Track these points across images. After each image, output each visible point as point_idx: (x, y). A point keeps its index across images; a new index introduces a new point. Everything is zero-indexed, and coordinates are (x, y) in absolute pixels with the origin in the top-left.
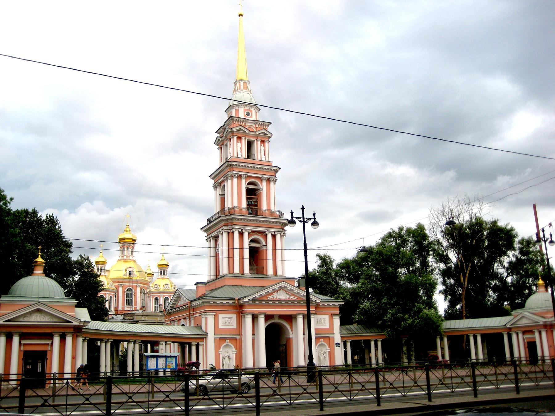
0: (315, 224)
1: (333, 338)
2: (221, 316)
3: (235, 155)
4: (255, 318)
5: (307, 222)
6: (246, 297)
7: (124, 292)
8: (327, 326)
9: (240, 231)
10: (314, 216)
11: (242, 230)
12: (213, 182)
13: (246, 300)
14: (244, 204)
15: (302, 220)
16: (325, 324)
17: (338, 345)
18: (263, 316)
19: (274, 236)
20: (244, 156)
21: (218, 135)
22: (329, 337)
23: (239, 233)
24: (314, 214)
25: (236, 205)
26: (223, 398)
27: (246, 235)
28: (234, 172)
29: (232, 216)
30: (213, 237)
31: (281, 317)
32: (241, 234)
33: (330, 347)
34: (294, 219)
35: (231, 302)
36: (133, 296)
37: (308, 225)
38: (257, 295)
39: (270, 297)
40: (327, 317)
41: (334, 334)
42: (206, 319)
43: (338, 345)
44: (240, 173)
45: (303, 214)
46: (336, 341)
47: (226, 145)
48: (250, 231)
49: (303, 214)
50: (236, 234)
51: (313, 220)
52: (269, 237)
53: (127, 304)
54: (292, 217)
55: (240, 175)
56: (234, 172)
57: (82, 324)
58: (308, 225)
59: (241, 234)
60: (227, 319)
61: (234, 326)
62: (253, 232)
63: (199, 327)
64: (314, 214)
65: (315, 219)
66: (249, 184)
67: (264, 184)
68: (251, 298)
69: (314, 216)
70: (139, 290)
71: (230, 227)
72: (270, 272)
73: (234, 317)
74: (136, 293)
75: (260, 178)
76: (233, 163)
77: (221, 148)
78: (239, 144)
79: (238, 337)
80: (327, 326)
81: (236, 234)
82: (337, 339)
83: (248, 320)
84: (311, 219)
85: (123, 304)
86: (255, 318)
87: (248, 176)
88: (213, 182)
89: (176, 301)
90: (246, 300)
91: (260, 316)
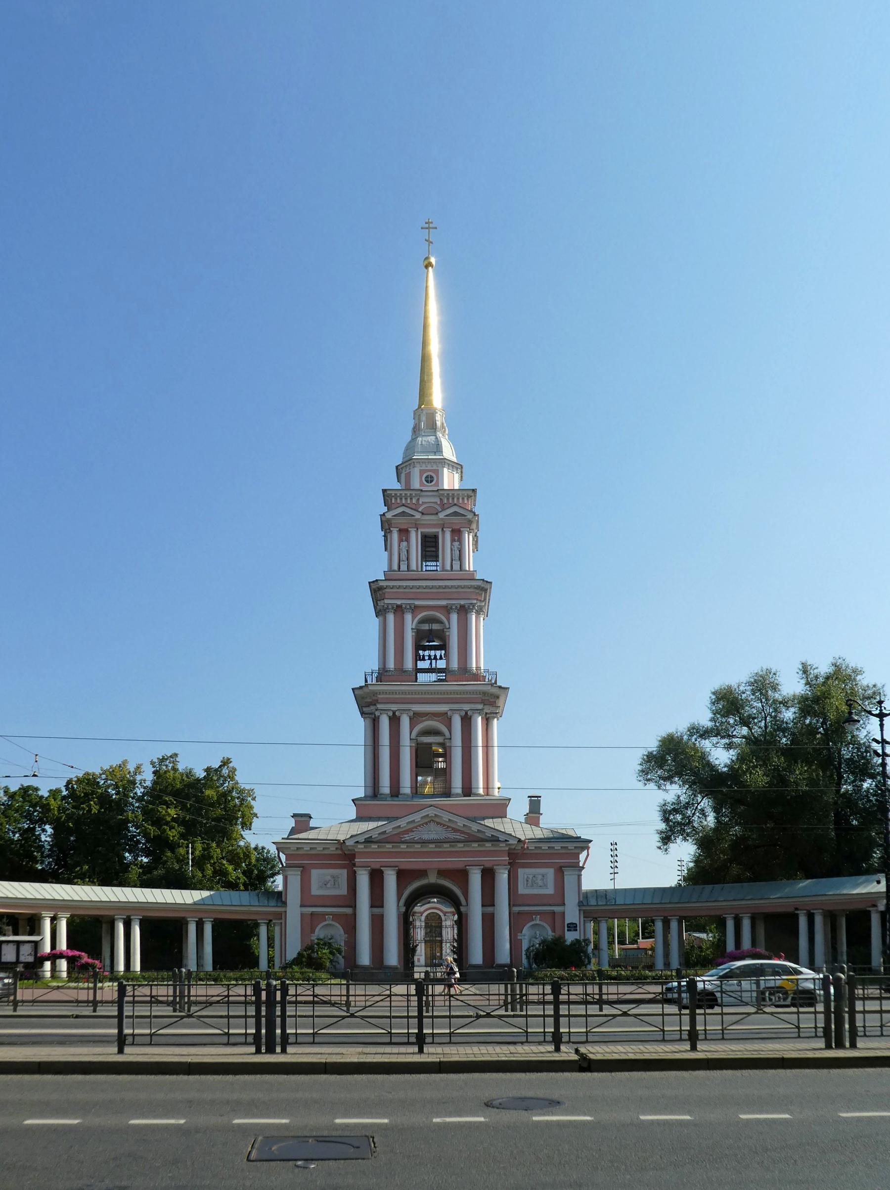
1: (563, 914)
2: (315, 873)
3: (395, 567)
8: (550, 890)
16: (545, 886)
22: (553, 913)
31: (442, 873)
32: (395, 720)
40: (550, 872)
44: (399, 602)
56: (386, 601)
60: (329, 878)
66: (422, 621)
67: (454, 617)
76: (381, 584)
79: (348, 911)
80: (550, 890)
87: (416, 607)
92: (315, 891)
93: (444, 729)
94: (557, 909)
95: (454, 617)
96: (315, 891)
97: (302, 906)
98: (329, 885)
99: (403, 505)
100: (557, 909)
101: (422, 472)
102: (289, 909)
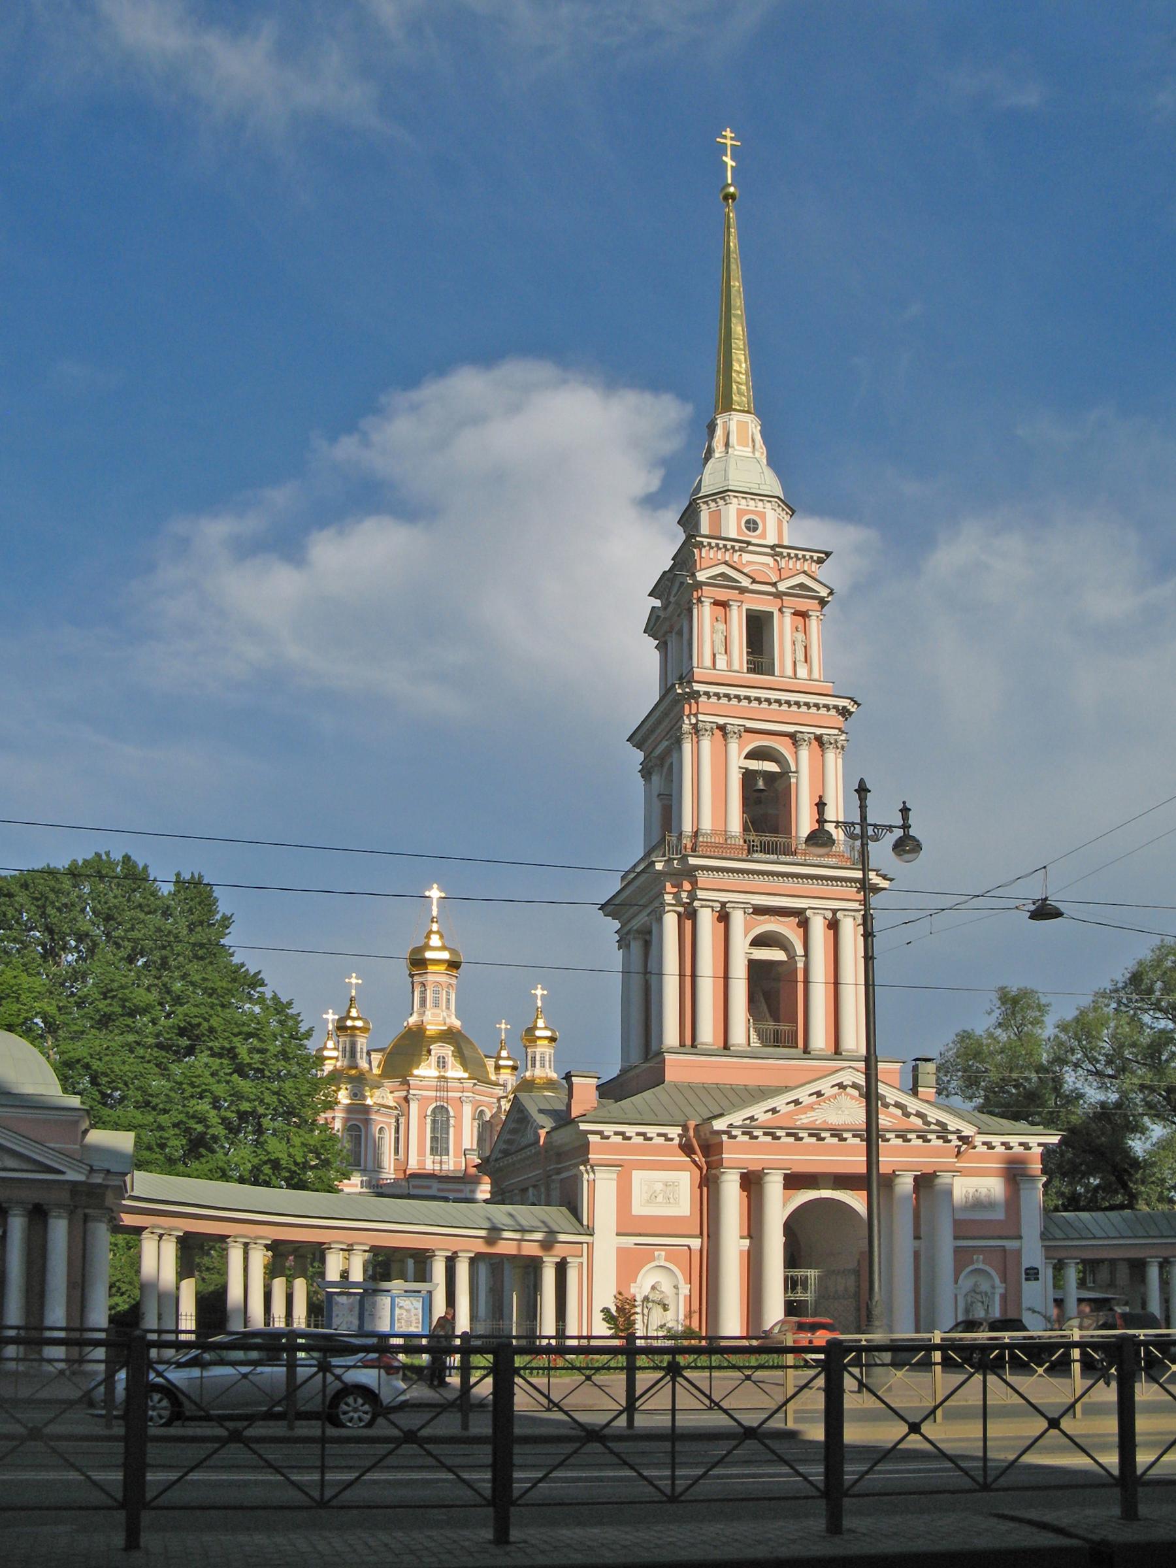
0: (906, 845)
1: (1018, 1252)
5: (876, 839)
6: (721, 1115)
10: (905, 818)
12: (640, 756)
14: (735, 824)
15: (858, 830)
17: (1032, 1274)
19: (833, 925)
20: (736, 667)
21: (658, 603)
22: (1003, 1249)
24: (905, 811)
26: (323, 1440)
27: (738, 919)
28: (701, 717)
29: (692, 861)
30: (638, 932)
32: (724, 917)
33: (1004, 1280)
34: (830, 827)
36: (452, 1130)
37: (881, 851)
39: (804, 1119)
41: (1020, 1237)
43: (1032, 1274)
45: (863, 808)
46: (1026, 1263)
47: (680, 633)
49: (863, 808)
50: (706, 918)
51: (899, 833)
52: (818, 926)
53: (433, 1151)
54: (821, 821)
55: (722, 728)
56: (701, 717)
57: (98, 1179)
58: (881, 851)
59: (724, 917)
62: (759, 911)
64: (905, 811)
65: (906, 827)
69: (905, 818)
70: (468, 1110)
72: (820, 1039)
75: (792, 736)
77: (666, 643)
78: (721, 626)
82: (1032, 1253)
84: (890, 828)
85: (421, 1152)
86: (752, 1183)
88: (640, 756)
90: (719, 1125)
91: (768, 1178)
92: (639, 1208)
93: (794, 937)
94: (1010, 1244)
95: (804, 753)
96: (639, 1208)
98: (660, 1199)
99: (726, 563)
100: (1010, 1244)
101: (741, 513)
102: (598, 1239)
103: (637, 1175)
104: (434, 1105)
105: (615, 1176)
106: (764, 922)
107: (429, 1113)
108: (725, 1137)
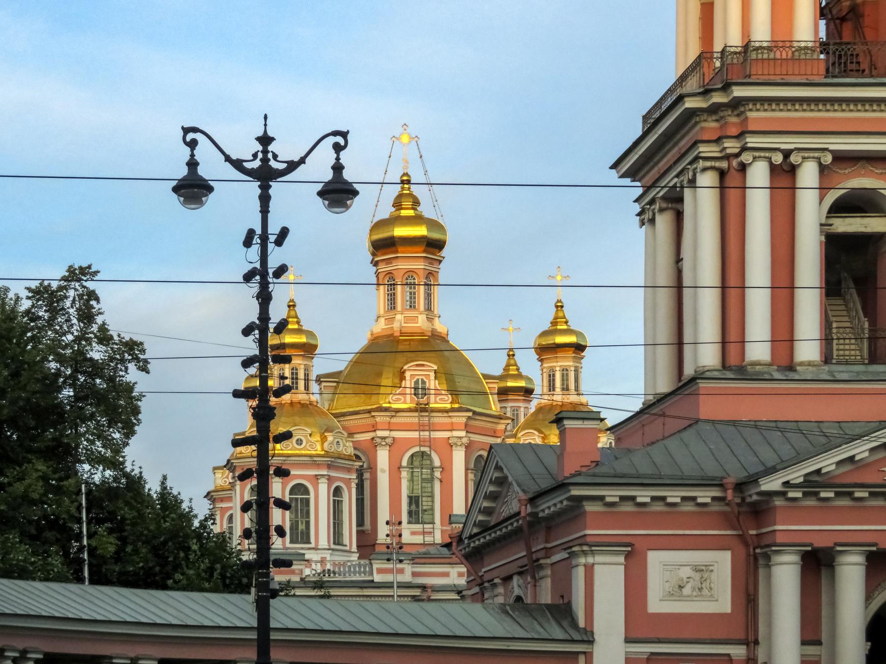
4: (818, 564)
7: (396, 469)
9: (778, 158)
11: (787, 154)
13: (771, 484)
18: (859, 559)
23: (774, 169)
25: (761, 33)
27: (808, 175)
29: (739, 92)
32: (784, 173)
35: (704, 496)
38: (827, 463)
42: (589, 570)
48: (828, 159)
50: (759, 174)
53: (414, 516)
59: (784, 173)
60: (686, 572)
61: (721, 601)
63: (562, 611)
68: (796, 475)
71: (732, 146)
73: (722, 563)
74: (447, 468)
81: (759, 174)
83: (785, 577)
86: (818, 564)
89: (493, 497)
90: (771, 484)
92: (657, 603)
96: (657, 603)
97: (628, 640)
98: (687, 591)
103: (656, 560)
104: (416, 449)
105: (621, 559)
106: (849, 177)
107: (404, 463)
108: (778, 502)
